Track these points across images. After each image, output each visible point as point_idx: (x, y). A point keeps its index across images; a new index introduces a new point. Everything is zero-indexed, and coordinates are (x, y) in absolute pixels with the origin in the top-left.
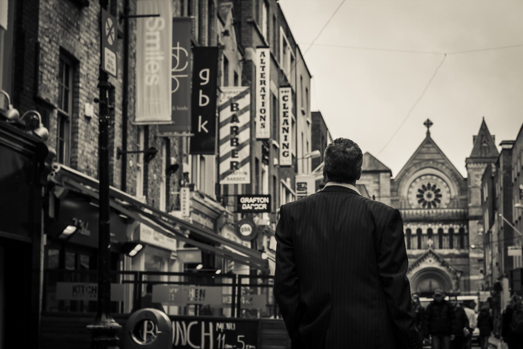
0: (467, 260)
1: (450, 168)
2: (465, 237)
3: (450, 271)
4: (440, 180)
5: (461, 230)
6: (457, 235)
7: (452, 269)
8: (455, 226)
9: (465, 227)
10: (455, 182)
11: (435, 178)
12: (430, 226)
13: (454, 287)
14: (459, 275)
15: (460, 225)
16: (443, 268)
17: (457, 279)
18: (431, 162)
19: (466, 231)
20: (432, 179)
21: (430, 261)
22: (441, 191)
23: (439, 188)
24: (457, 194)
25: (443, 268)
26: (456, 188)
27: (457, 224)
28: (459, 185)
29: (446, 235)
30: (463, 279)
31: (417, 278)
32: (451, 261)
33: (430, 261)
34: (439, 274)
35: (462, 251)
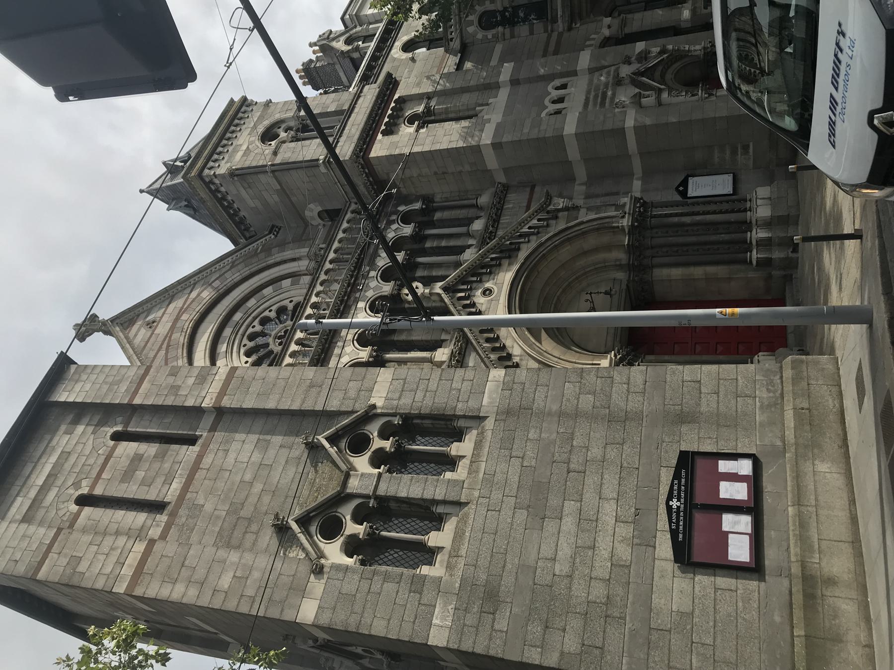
0: (511, 197)
1: (228, 267)
3: (537, 231)
4: (252, 302)
5: (406, 219)
7: (535, 222)
10: (270, 255)
11: (238, 316)
16: (522, 255)
18: (185, 317)
20: (238, 326)
22: (286, 303)
23: (274, 308)
24: (304, 251)
25: (522, 255)
26: (288, 254)
28: (282, 246)
33: (487, 292)
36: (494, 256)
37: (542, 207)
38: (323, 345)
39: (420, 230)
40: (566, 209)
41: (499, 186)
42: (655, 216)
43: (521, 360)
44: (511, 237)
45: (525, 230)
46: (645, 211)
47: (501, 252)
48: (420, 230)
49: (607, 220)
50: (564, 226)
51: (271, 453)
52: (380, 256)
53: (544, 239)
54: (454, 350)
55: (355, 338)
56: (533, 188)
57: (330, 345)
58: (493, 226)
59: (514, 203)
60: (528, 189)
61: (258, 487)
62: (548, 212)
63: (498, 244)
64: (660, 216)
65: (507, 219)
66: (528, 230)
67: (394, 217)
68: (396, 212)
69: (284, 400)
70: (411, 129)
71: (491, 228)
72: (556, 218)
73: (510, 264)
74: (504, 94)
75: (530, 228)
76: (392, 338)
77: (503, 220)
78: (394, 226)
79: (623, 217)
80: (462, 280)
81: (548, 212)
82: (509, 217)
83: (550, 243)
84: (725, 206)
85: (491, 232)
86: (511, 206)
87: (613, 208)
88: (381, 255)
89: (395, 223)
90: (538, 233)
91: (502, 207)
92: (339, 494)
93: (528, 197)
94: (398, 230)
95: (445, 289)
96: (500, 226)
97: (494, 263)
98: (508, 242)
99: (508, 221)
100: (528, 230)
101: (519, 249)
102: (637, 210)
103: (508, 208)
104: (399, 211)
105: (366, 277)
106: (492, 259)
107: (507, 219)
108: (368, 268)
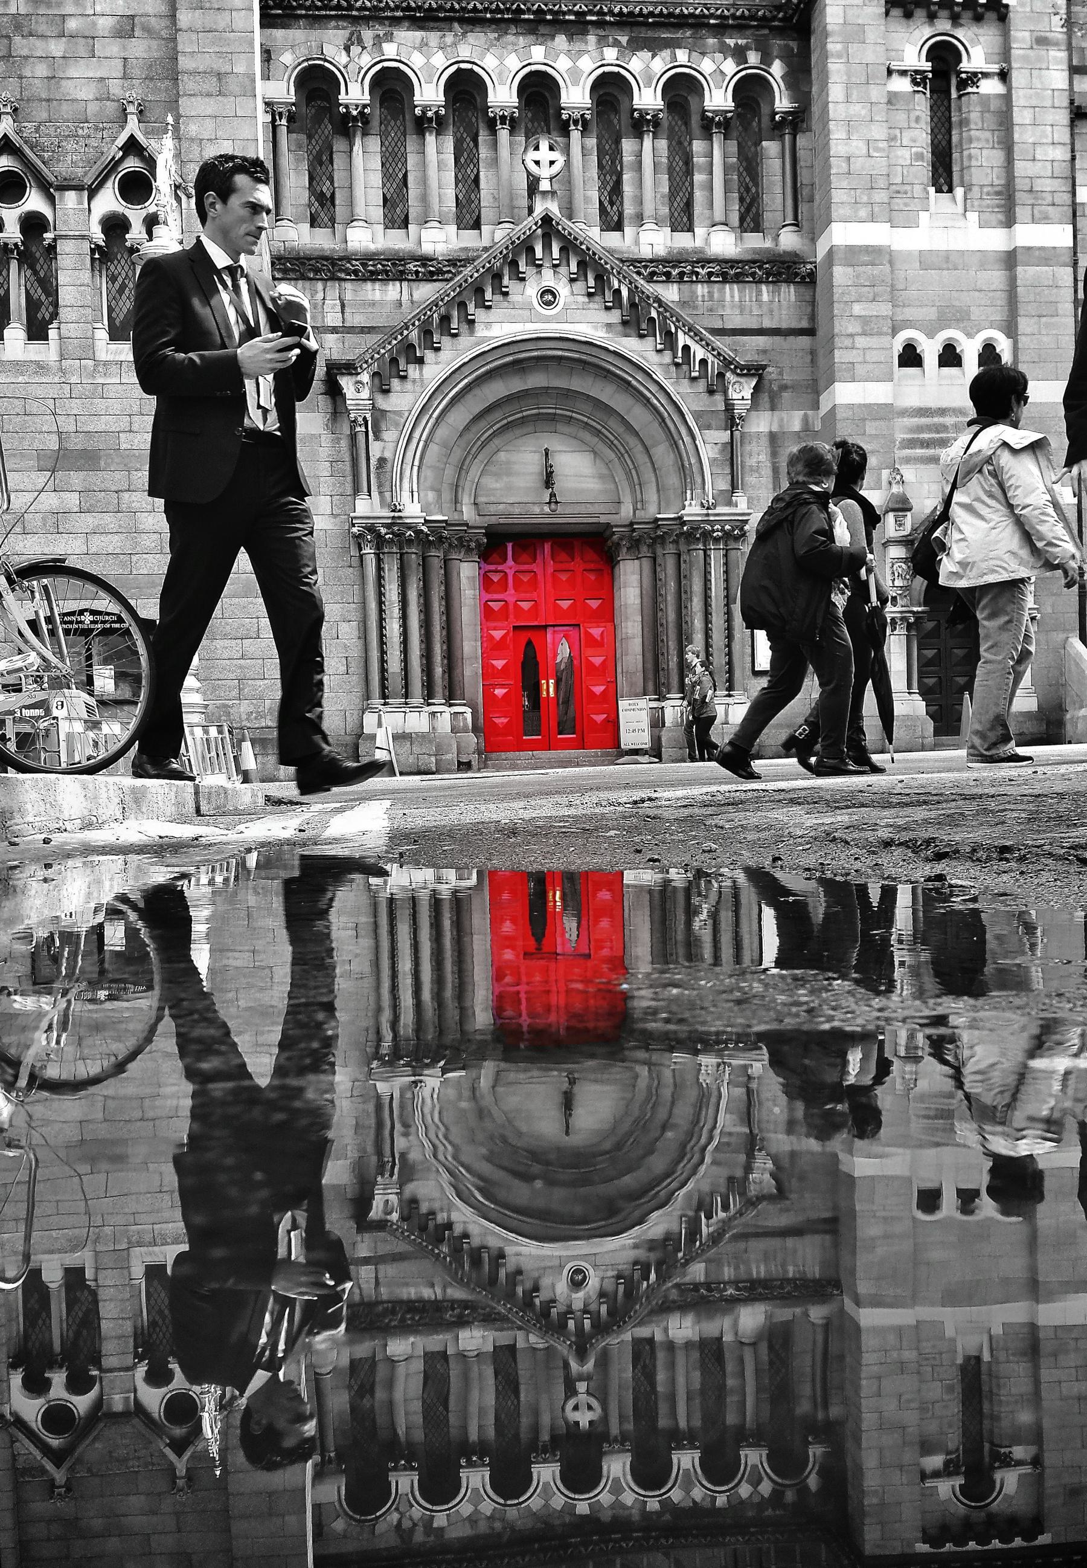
0: (789, 293)
2: (771, 147)
6: (724, 124)
7: (699, 352)
8: (707, 66)
9: (777, 69)
12: (538, 53)
13: (714, 482)
14: (741, 391)
15: (739, 54)
16: (631, 346)
17: (731, 420)
19: (783, 103)
21: (548, 296)
25: (631, 346)
27: (724, 50)
29: (640, 125)
30: (761, 424)
31: (460, 417)
32: (683, 303)
33: (548, 296)
34: (605, 393)
35: (755, 241)
36: (625, 293)
37: (731, 363)
38: (441, 8)
39: (719, 125)
40: (729, 407)
41: (809, 266)
42: (706, 556)
43: (414, 381)
44: (665, 318)
45: (682, 339)
46: (717, 540)
47: (633, 305)
48: (719, 125)
49: (699, 480)
50: (685, 409)
51: (113, 48)
52: (653, 57)
53: (659, 376)
54: (435, 263)
55: (463, 66)
56: (810, 332)
57: (445, 19)
58: (710, 274)
59: (771, 302)
60: (804, 324)
61: (56, 48)
62: (721, 375)
63: (648, 297)
64: (707, 564)
65: (732, 297)
66: (681, 345)
67: (753, 58)
68: (767, 60)
69: (194, 36)
70: (915, 58)
71: (706, 270)
72: (711, 392)
73: (609, 326)
74: (996, 240)
75: (686, 348)
76: (481, 132)
77: (731, 290)
78: (730, 66)
79: (702, 505)
80: (570, 246)
81: (721, 375)
82: (737, 299)
83: (653, 388)
84: (719, 659)
85: (697, 274)
86: (765, 297)
87: (724, 485)
88: (657, 59)
89: (738, 64)
90: (677, 365)
91: (760, 282)
92: (51, 185)
93: (784, 325)
94: (720, 78)
95: (547, 220)
96: (717, 286)
97: (609, 296)
98: (654, 314)
99: (728, 297)
100: (681, 345)
101: (642, 336)
102: (717, 527)
103: (759, 293)
104: (770, 65)
105: (602, 42)
106: (618, 292)
107: (732, 297)
108: (624, 40)
